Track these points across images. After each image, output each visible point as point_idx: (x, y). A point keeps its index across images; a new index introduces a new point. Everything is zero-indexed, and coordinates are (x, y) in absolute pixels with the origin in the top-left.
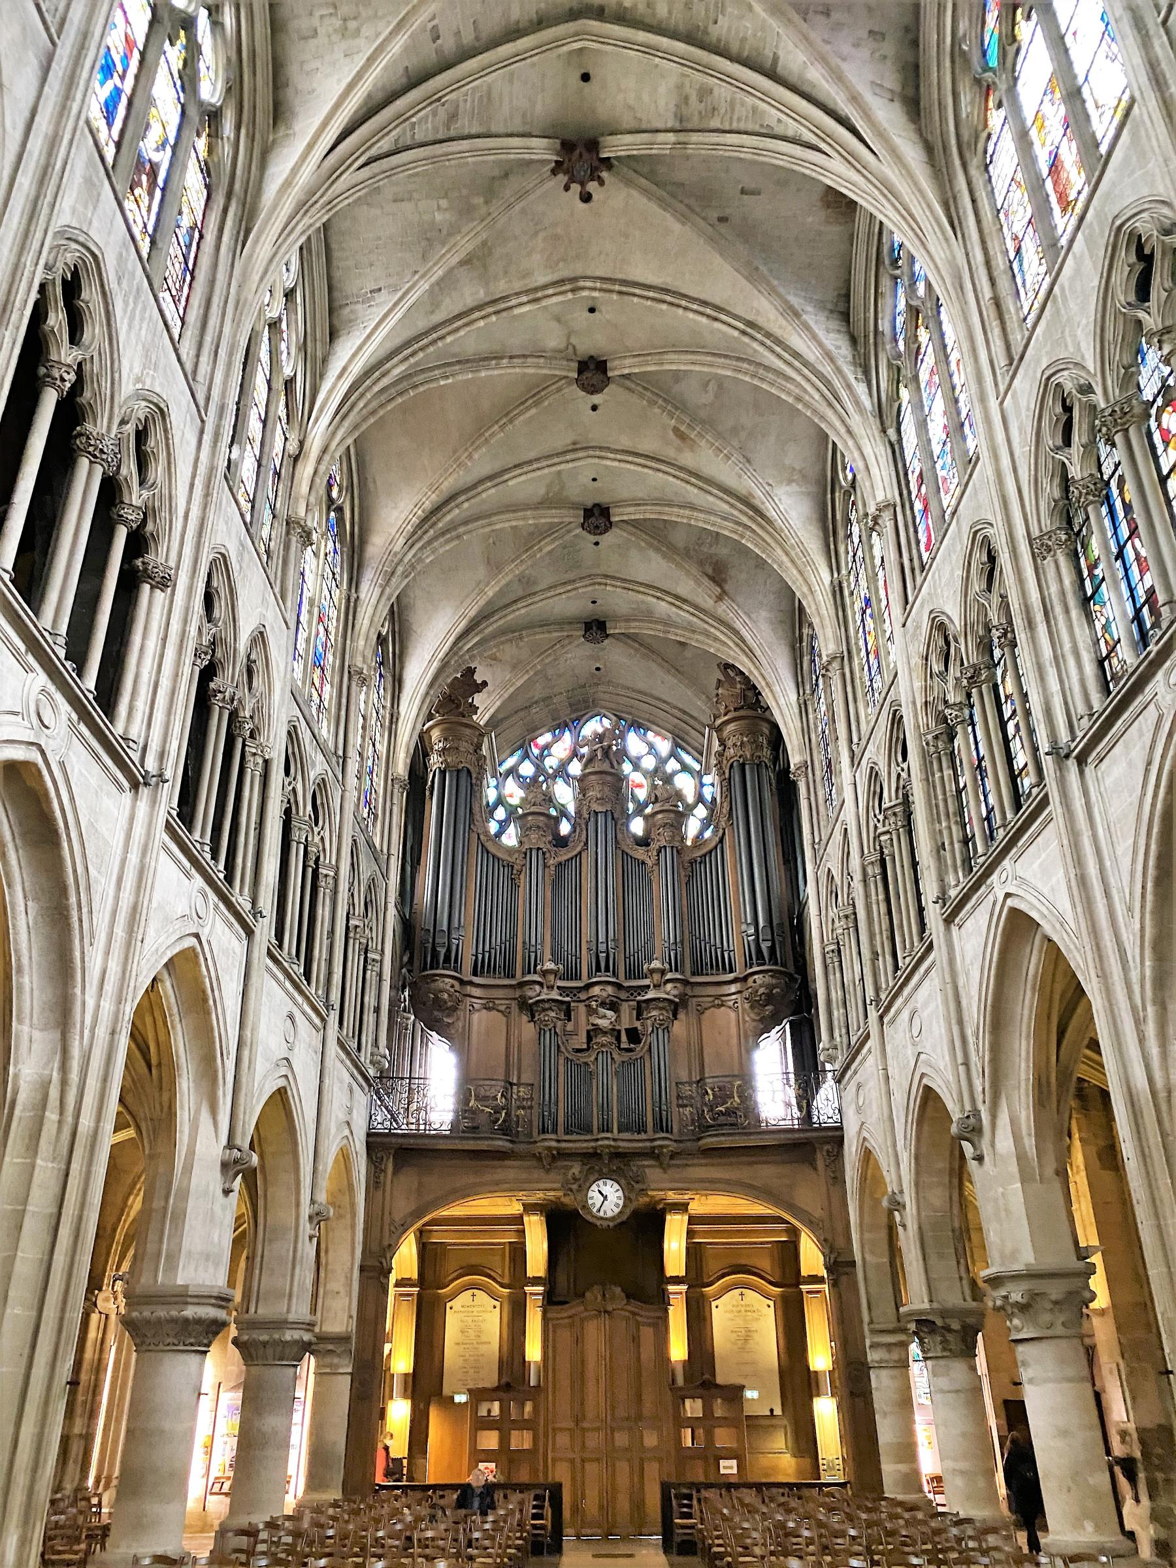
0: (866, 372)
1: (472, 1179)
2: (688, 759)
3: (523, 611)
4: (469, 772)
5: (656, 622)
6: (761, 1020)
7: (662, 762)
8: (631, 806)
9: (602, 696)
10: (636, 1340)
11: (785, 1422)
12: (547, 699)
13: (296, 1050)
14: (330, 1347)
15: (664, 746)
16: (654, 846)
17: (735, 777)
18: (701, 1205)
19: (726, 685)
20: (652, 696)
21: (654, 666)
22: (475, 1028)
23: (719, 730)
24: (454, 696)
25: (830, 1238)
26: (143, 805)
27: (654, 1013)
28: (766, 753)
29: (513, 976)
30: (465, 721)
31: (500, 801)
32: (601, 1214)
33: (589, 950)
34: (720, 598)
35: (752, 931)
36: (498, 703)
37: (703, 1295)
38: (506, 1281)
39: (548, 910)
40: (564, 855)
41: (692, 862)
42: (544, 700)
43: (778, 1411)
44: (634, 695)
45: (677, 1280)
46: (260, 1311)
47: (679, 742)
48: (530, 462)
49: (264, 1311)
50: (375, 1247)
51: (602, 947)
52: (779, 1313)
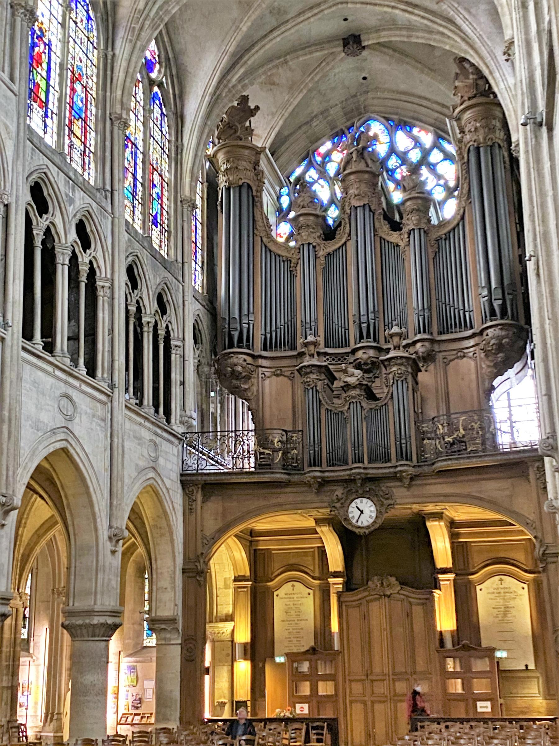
1: (262, 503)
3: (278, 39)
4: (249, 186)
5: (400, 29)
6: (495, 366)
7: (426, 153)
9: (370, 102)
10: (409, 615)
11: (538, 675)
12: (324, 112)
13: (77, 420)
14: (163, 626)
15: (427, 139)
16: (405, 230)
17: (471, 160)
18: (462, 513)
19: (461, 77)
20: (413, 95)
21: (409, 68)
22: (267, 390)
23: (458, 119)
24: (234, 124)
25: (539, 535)
27: (394, 369)
29: (295, 348)
30: (241, 143)
32: (359, 524)
33: (354, 322)
35: (485, 292)
36: (281, 123)
37: (470, 582)
38: (317, 574)
39: (321, 294)
40: (332, 246)
42: (322, 113)
43: (532, 667)
44: (398, 96)
45: (445, 571)
46: (75, 605)
47: (440, 134)
49: (79, 605)
50: (192, 556)
51: (364, 319)
52: (532, 594)
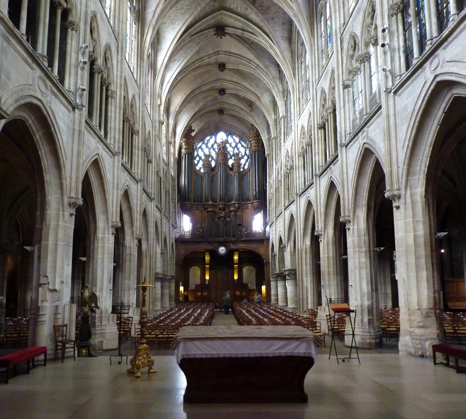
0: (282, 81)
2: (243, 143)
8: (229, 156)
15: (237, 140)
23: (250, 141)
28: (261, 148)
31: (198, 155)
34: (251, 111)
41: (243, 175)
47: (241, 139)
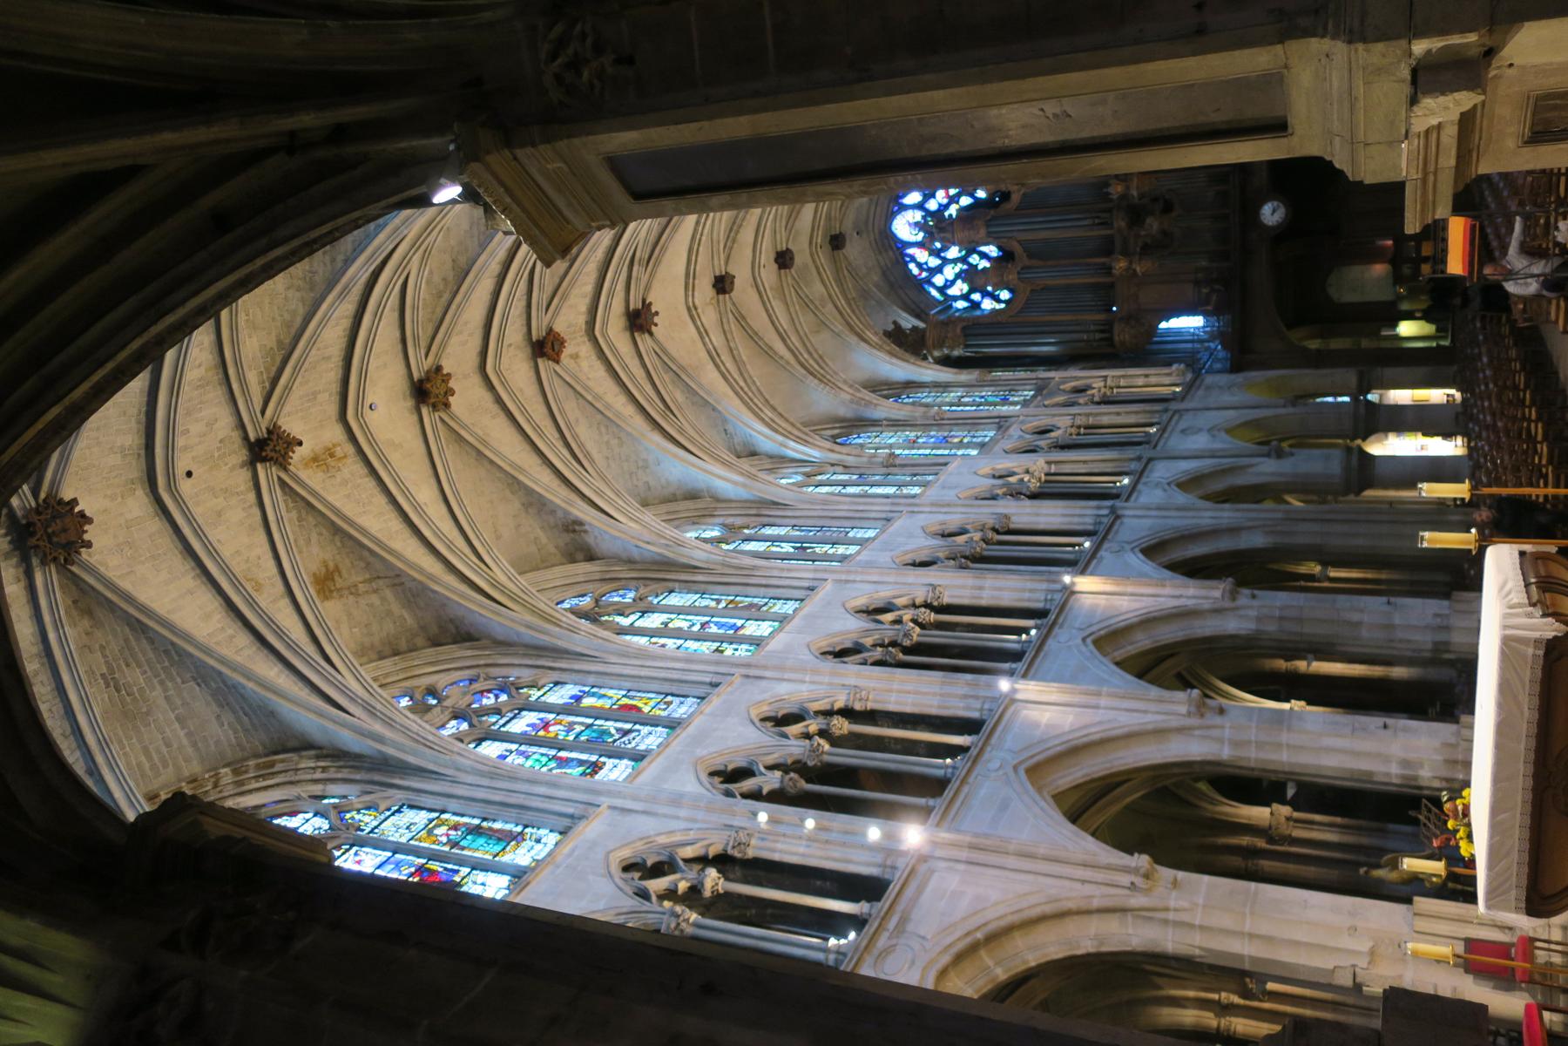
26: (1127, 512)
31: (965, 297)
48: (770, 316)
